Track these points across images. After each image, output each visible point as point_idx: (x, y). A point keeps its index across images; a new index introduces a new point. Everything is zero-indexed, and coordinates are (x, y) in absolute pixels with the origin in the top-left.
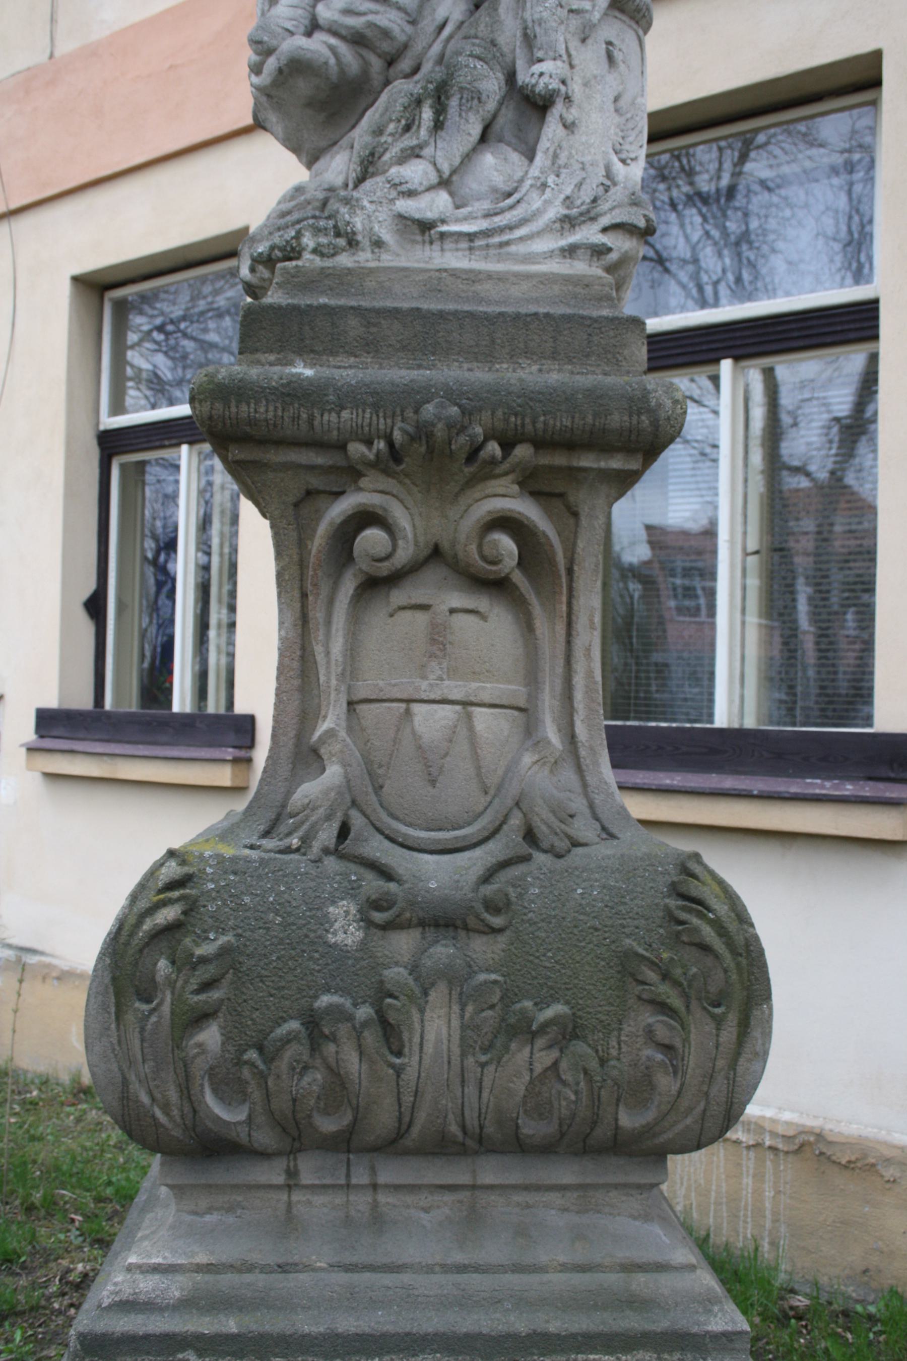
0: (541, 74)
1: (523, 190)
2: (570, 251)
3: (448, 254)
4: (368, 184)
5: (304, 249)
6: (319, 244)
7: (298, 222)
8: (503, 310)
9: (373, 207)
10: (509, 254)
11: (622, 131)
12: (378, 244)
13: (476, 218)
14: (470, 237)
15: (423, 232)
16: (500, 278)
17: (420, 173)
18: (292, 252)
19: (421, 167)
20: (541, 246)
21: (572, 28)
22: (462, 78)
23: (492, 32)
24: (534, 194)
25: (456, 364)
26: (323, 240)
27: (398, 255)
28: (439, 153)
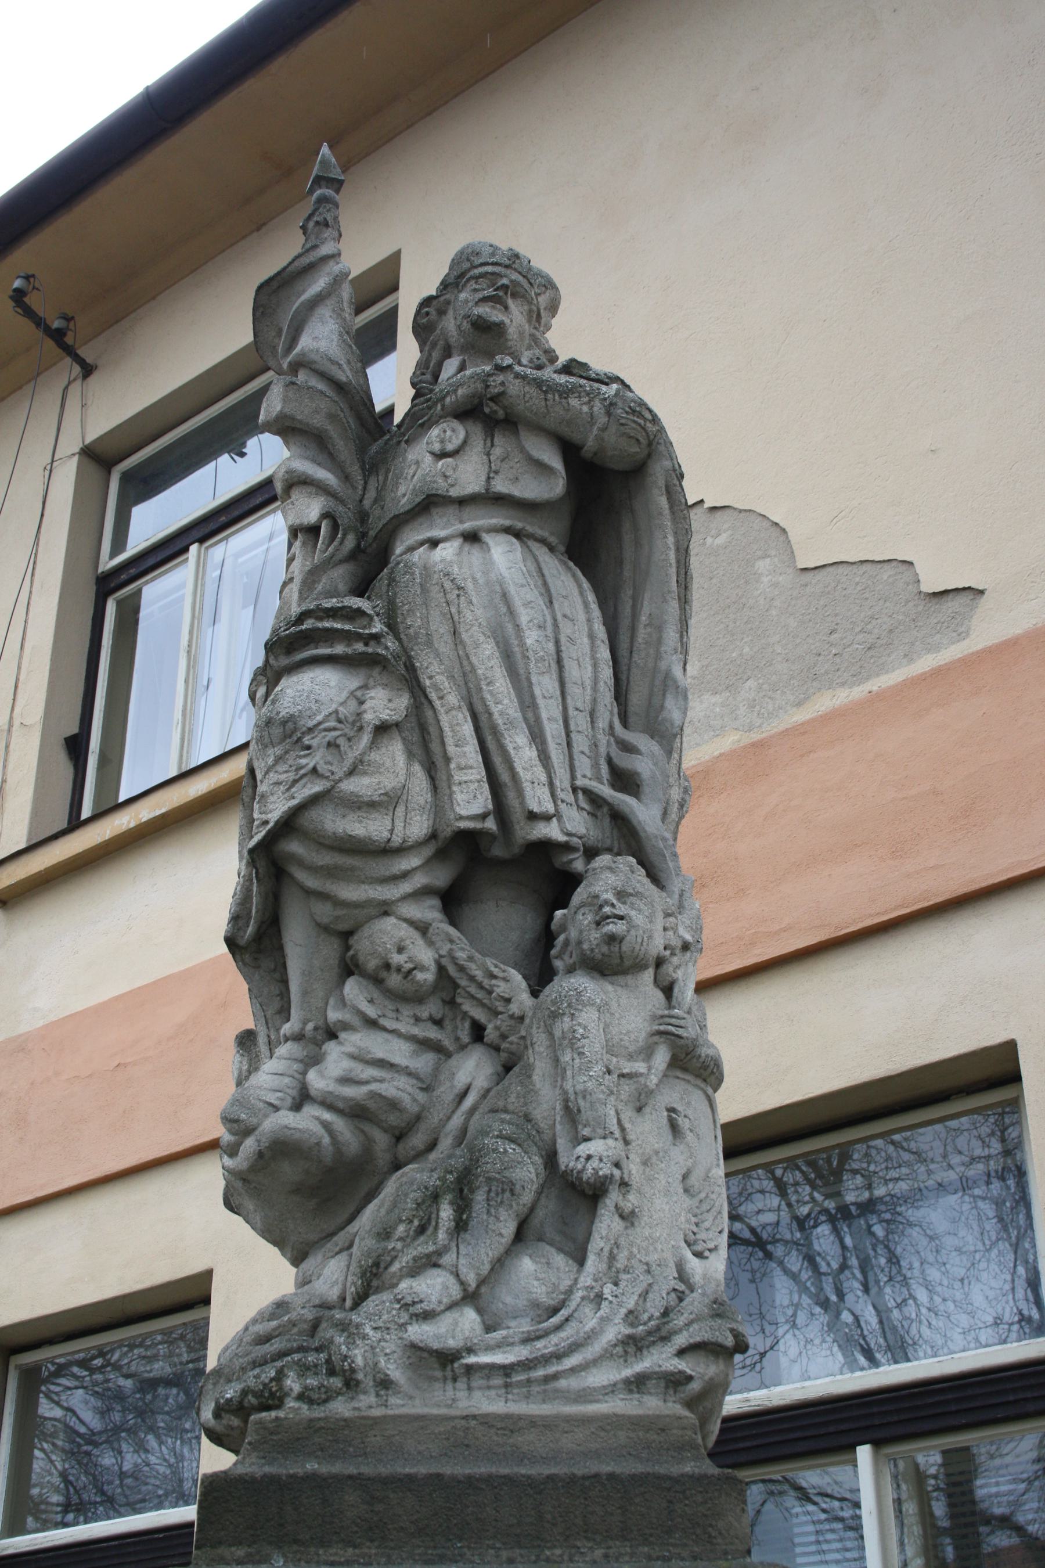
0: (589, 1157)
1: (573, 1304)
2: (638, 1383)
3: (477, 1394)
4: (371, 1304)
5: (287, 1395)
6: (306, 1388)
7: (282, 1354)
8: (554, 1470)
9: (379, 1335)
10: (556, 1391)
11: (695, 1216)
12: (385, 1384)
13: (512, 1344)
14: (506, 1370)
15: (443, 1366)
16: (545, 1424)
17: (438, 1287)
18: (271, 1398)
19: (440, 1280)
20: (600, 1377)
21: (624, 1096)
22: (490, 1165)
23: (526, 1104)
24: (588, 1310)
25: (492, 1552)
26: (312, 1381)
27: (411, 1398)
28: (462, 1261)
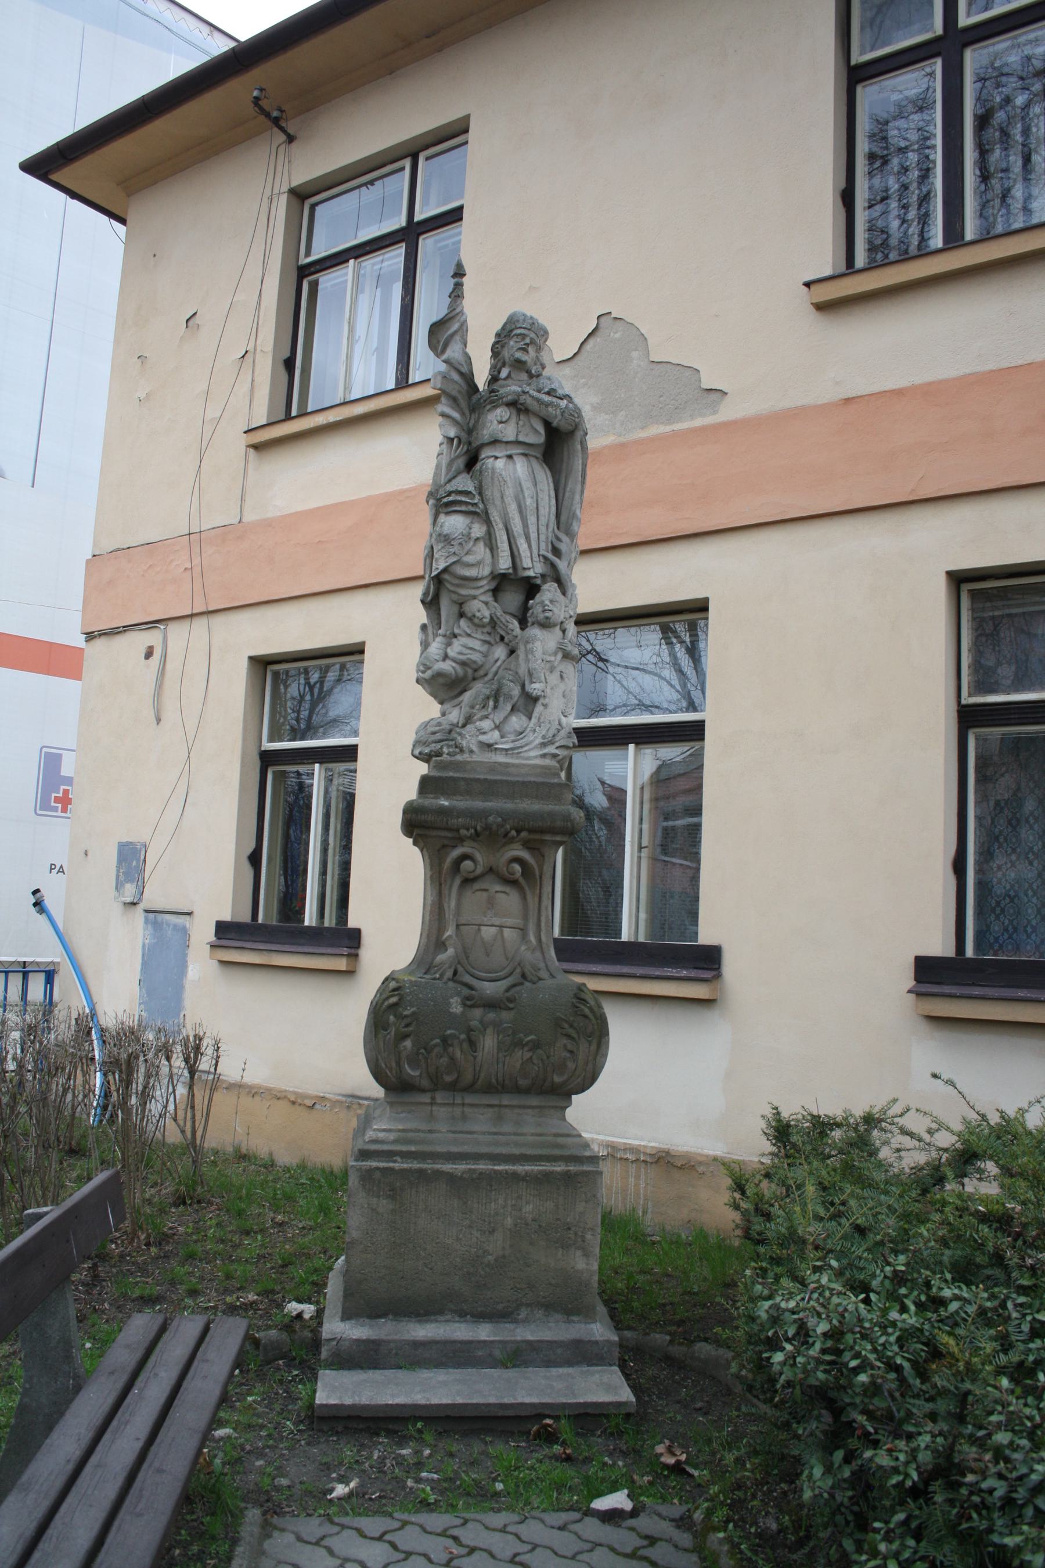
2: (544, 756)
12: (471, 752)
14: (506, 750)
20: (532, 754)
22: (505, 690)
